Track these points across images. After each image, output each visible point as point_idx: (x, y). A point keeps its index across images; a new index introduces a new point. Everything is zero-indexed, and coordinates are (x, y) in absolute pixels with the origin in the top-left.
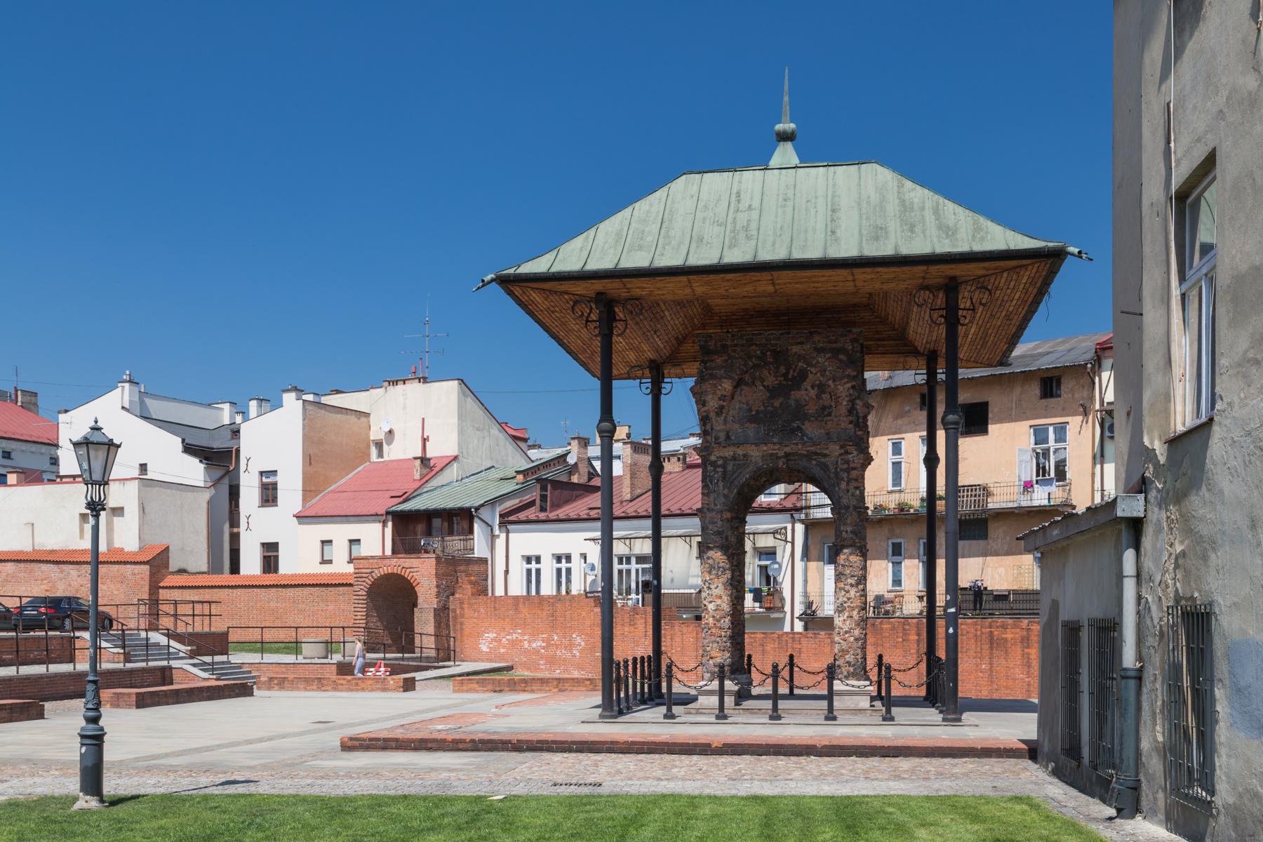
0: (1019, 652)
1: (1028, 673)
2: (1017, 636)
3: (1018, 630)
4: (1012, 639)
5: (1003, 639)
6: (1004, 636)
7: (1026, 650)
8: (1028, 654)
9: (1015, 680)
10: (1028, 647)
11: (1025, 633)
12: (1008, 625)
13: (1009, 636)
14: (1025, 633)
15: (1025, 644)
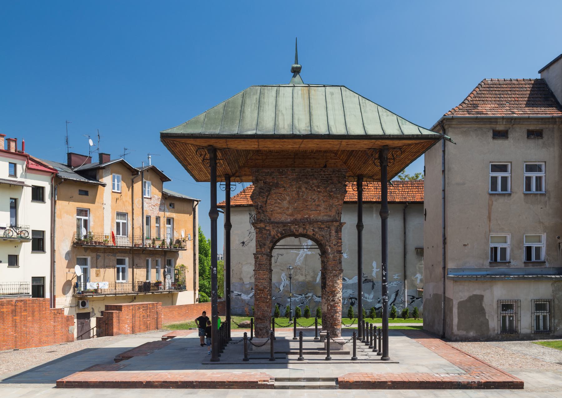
0: (11, 319)
1: (15, 330)
2: (10, 309)
3: (10, 306)
4: (7, 312)
5: (2, 312)
6: (2, 310)
7: (14, 318)
8: (16, 320)
9: (8, 336)
10: (15, 316)
11: (13, 308)
12: (4, 303)
13: (5, 310)
14: (13, 308)
15: (14, 314)
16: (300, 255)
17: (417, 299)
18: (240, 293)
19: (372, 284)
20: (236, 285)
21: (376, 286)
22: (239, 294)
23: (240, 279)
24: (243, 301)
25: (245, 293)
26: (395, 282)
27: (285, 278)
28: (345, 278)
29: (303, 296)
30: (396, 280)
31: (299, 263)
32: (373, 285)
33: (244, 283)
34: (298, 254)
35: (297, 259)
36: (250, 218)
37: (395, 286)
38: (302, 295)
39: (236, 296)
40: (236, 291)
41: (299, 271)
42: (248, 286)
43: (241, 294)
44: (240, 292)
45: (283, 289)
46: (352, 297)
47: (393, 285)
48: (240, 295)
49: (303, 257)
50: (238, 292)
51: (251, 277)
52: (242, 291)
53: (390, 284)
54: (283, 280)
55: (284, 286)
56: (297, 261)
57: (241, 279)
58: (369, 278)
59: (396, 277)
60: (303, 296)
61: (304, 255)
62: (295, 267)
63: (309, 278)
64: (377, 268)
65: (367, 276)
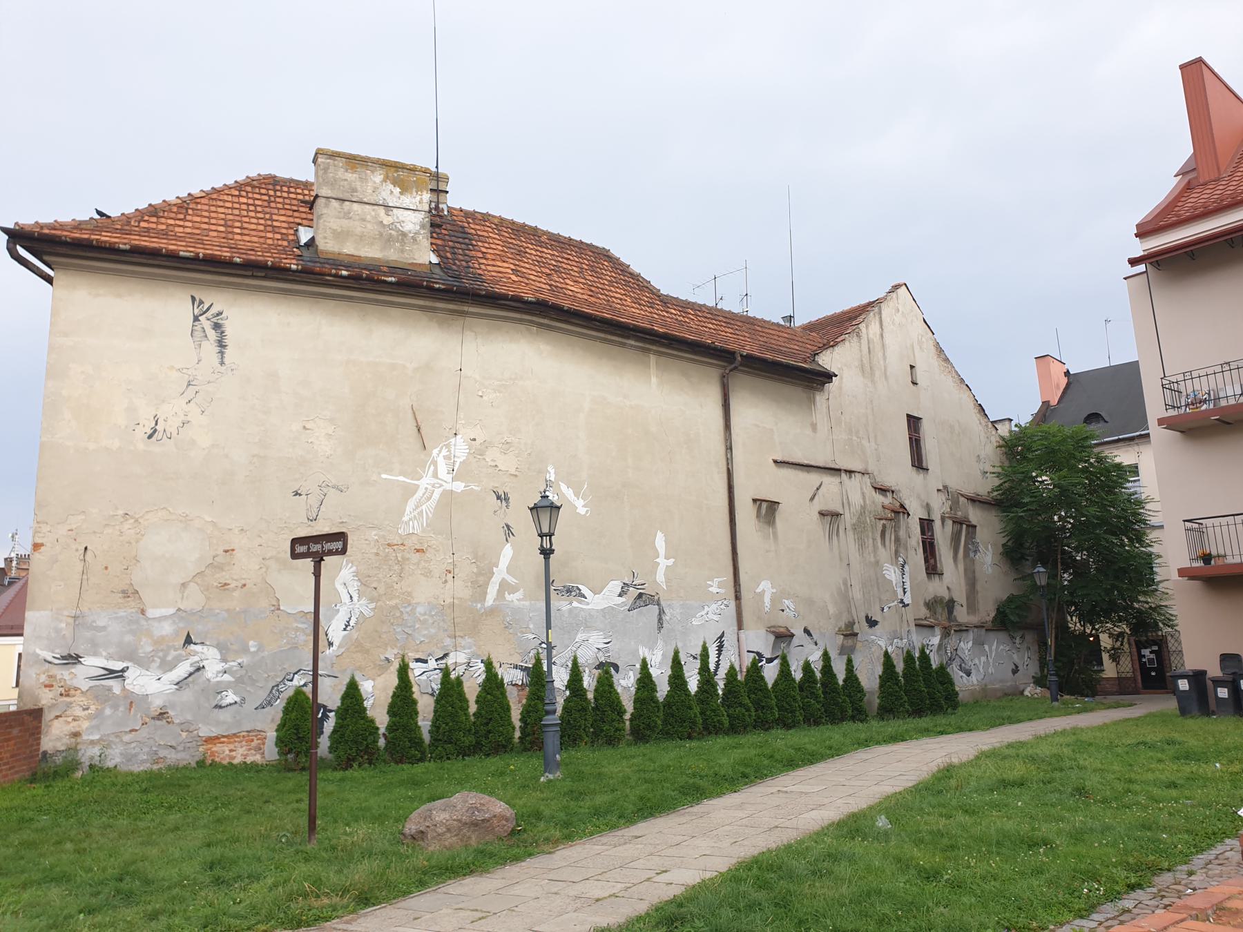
16: (420, 493)
17: (770, 661)
18: (118, 666)
19: (657, 612)
20: (100, 623)
21: (667, 618)
22: (111, 671)
23: (124, 592)
24: (132, 701)
25: (143, 663)
26: (714, 606)
27: (354, 587)
28: (580, 587)
29: (432, 664)
30: (715, 598)
31: (415, 527)
32: (660, 614)
33: (143, 612)
34: (410, 491)
35: (408, 509)
36: (196, 319)
37: (716, 618)
38: (425, 662)
39: (91, 678)
40: (96, 654)
41: (415, 557)
42: (167, 629)
43: (123, 671)
44: (122, 659)
45: (344, 637)
46: (602, 659)
47: (711, 616)
48: (119, 675)
49: (432, 503)
50: (110, 657)
51: (184, 585)
52: (130, 655)
53: (703, 613)
54: (346, 599)
55: (347, 626)
56: (405, 519)
57: (130, 593)
58: (648, 590)
59: (714, 590)
60: (432, 664)
61: (436, 496)
62: (397, 540)
63: (459, 589)
64: (667, 558)
65: (643, 582)
